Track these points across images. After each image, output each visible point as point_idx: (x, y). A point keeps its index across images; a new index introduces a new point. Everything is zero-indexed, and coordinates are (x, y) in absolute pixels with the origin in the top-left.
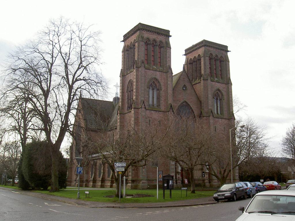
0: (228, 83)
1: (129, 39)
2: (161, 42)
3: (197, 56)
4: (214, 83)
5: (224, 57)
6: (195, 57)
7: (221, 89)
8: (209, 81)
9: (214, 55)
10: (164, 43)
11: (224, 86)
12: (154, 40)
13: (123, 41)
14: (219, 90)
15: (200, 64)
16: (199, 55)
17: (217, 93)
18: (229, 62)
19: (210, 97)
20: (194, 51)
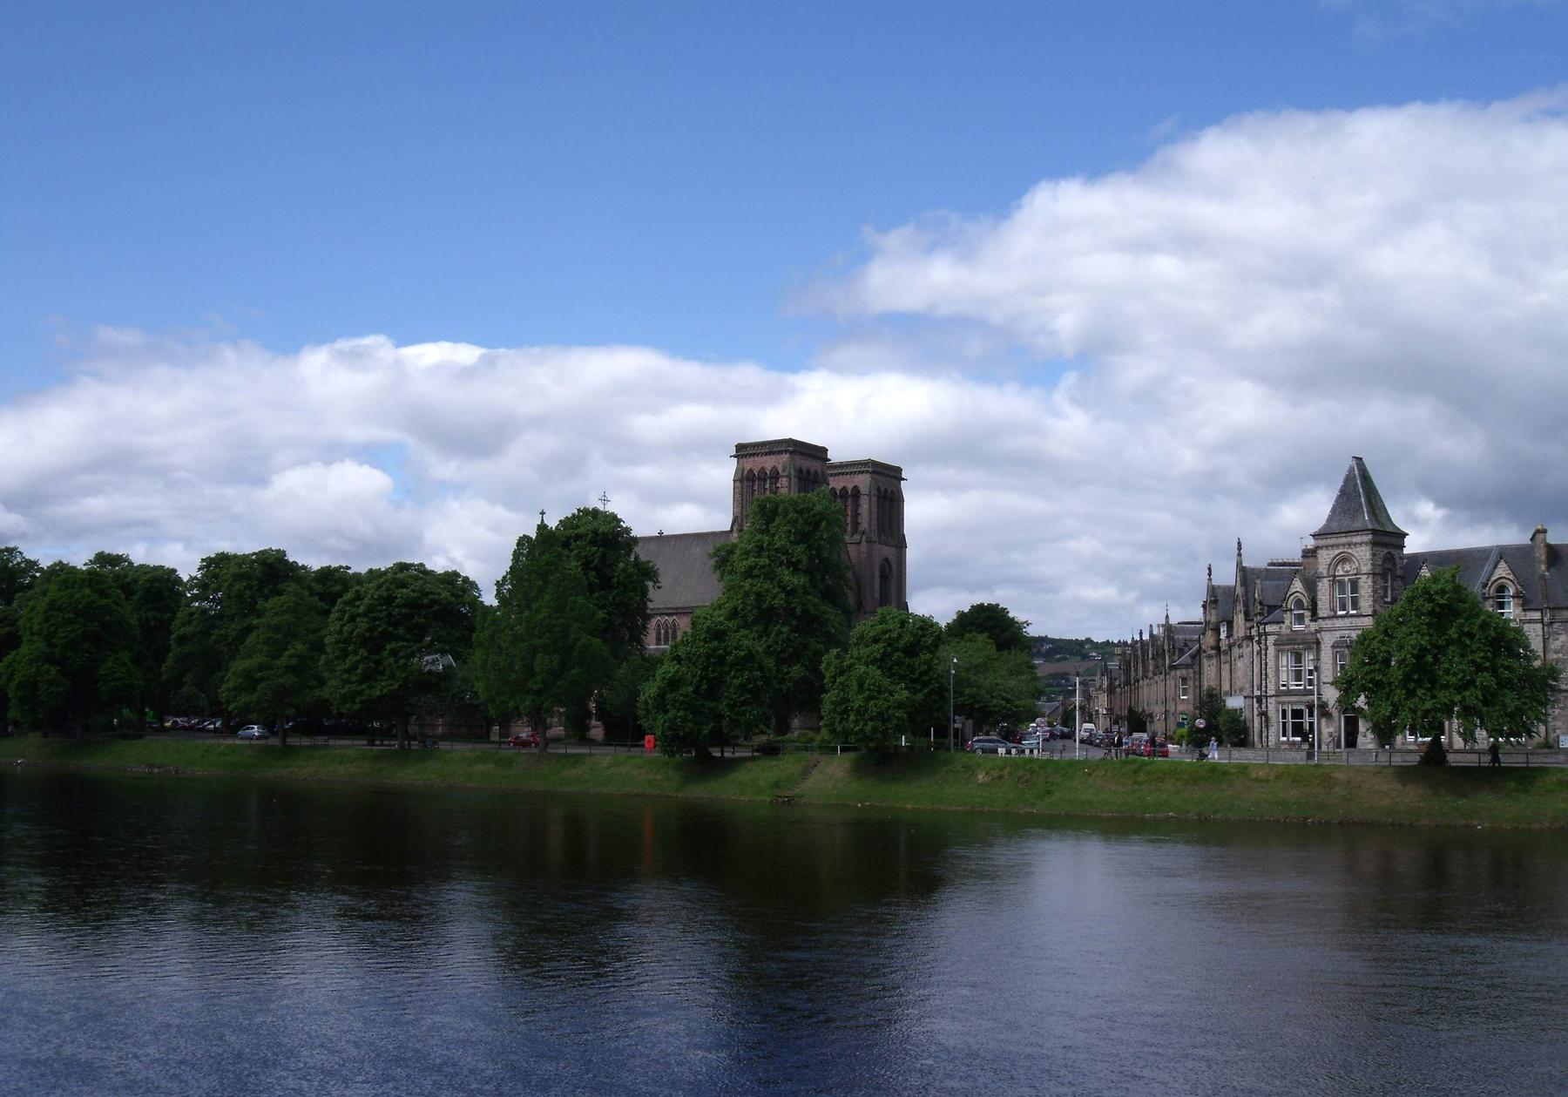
0: (901, 544)
1: (757, 459)
2: (816, 472)
3: (850, 486)
4: (881, 546)
5: (895, 490)
6: (844, 487)
7: (890, 557)
8: (877, 543)
9: (883, 489)
10: (820, 476)
11: (893, 550)
12: (808, 471)
13: (734, 456)
14: (887, 560)
15: (857, 505)
16: (856, 486)
17: (883, 564)
18: (903, 501)
19: (877, 573)
20: (843, 474)
